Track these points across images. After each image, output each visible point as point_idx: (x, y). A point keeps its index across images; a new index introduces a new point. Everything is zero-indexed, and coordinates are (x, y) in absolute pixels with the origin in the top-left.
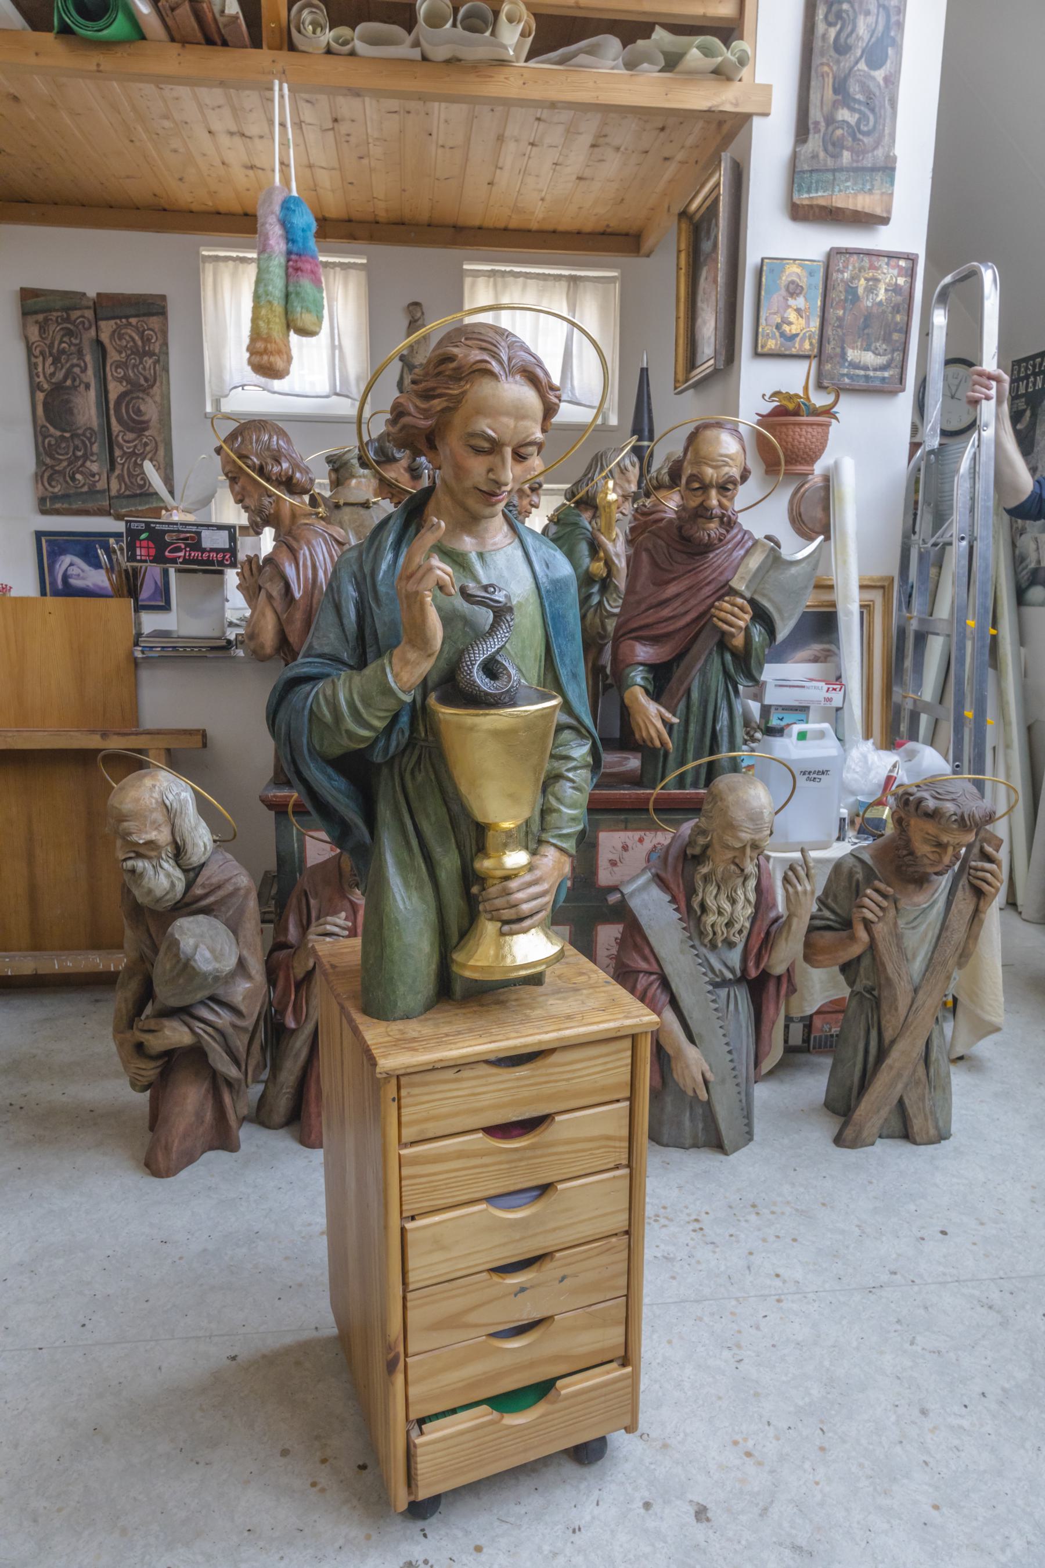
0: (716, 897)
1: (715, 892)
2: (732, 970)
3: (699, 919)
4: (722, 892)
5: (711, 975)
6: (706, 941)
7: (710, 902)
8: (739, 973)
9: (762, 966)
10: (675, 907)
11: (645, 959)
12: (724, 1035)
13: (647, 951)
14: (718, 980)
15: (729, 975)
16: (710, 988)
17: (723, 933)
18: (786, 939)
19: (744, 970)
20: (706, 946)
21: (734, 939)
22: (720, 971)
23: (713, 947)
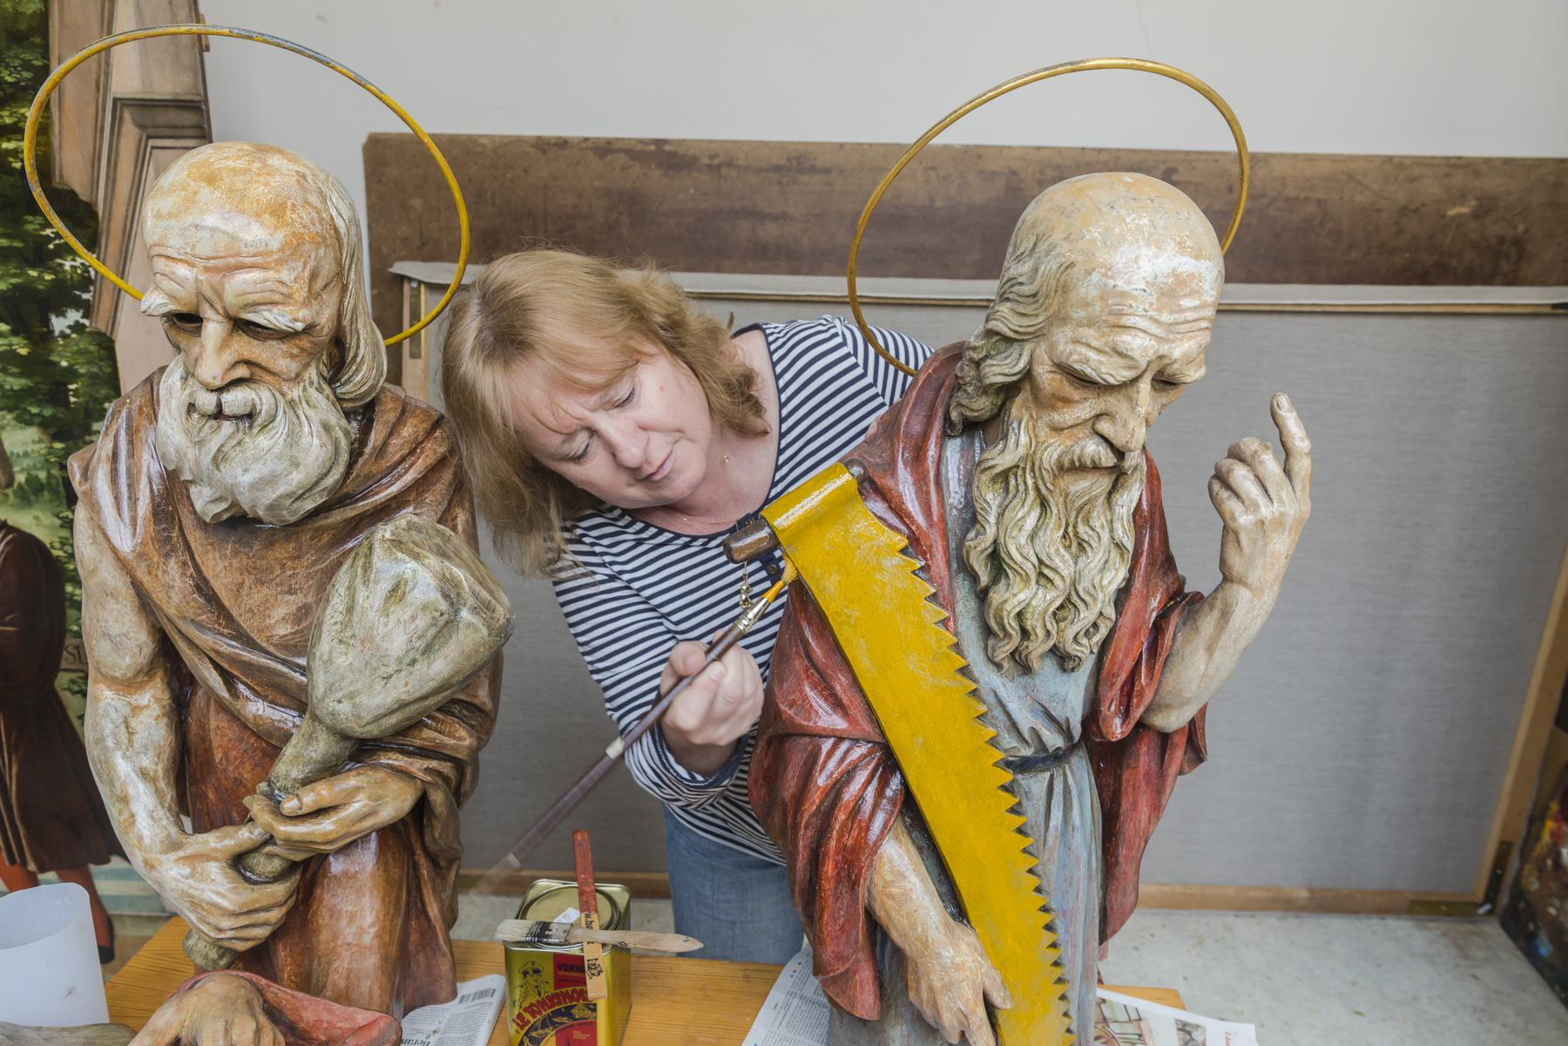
0: (1033, 536)
1: (1030, 522)
3: (982, 596)
4: (1052, 521)
5: (1009, 741)
6: (1003, 652)
7: (1017, 548)
8: (1077, 731)
9: (1137, 714)
10: (919, 564)
11: (838, 705)
12: (1038, 890)
13: (841, 684)
14: (1028, 752)
15: (1054, 741)
16: (1007, 776)
17: (1048, 633)
18: (1210, 649)
19: (1092, 717)
20: (998, 666)
21: (1072, 649)
23: (1024, 667)
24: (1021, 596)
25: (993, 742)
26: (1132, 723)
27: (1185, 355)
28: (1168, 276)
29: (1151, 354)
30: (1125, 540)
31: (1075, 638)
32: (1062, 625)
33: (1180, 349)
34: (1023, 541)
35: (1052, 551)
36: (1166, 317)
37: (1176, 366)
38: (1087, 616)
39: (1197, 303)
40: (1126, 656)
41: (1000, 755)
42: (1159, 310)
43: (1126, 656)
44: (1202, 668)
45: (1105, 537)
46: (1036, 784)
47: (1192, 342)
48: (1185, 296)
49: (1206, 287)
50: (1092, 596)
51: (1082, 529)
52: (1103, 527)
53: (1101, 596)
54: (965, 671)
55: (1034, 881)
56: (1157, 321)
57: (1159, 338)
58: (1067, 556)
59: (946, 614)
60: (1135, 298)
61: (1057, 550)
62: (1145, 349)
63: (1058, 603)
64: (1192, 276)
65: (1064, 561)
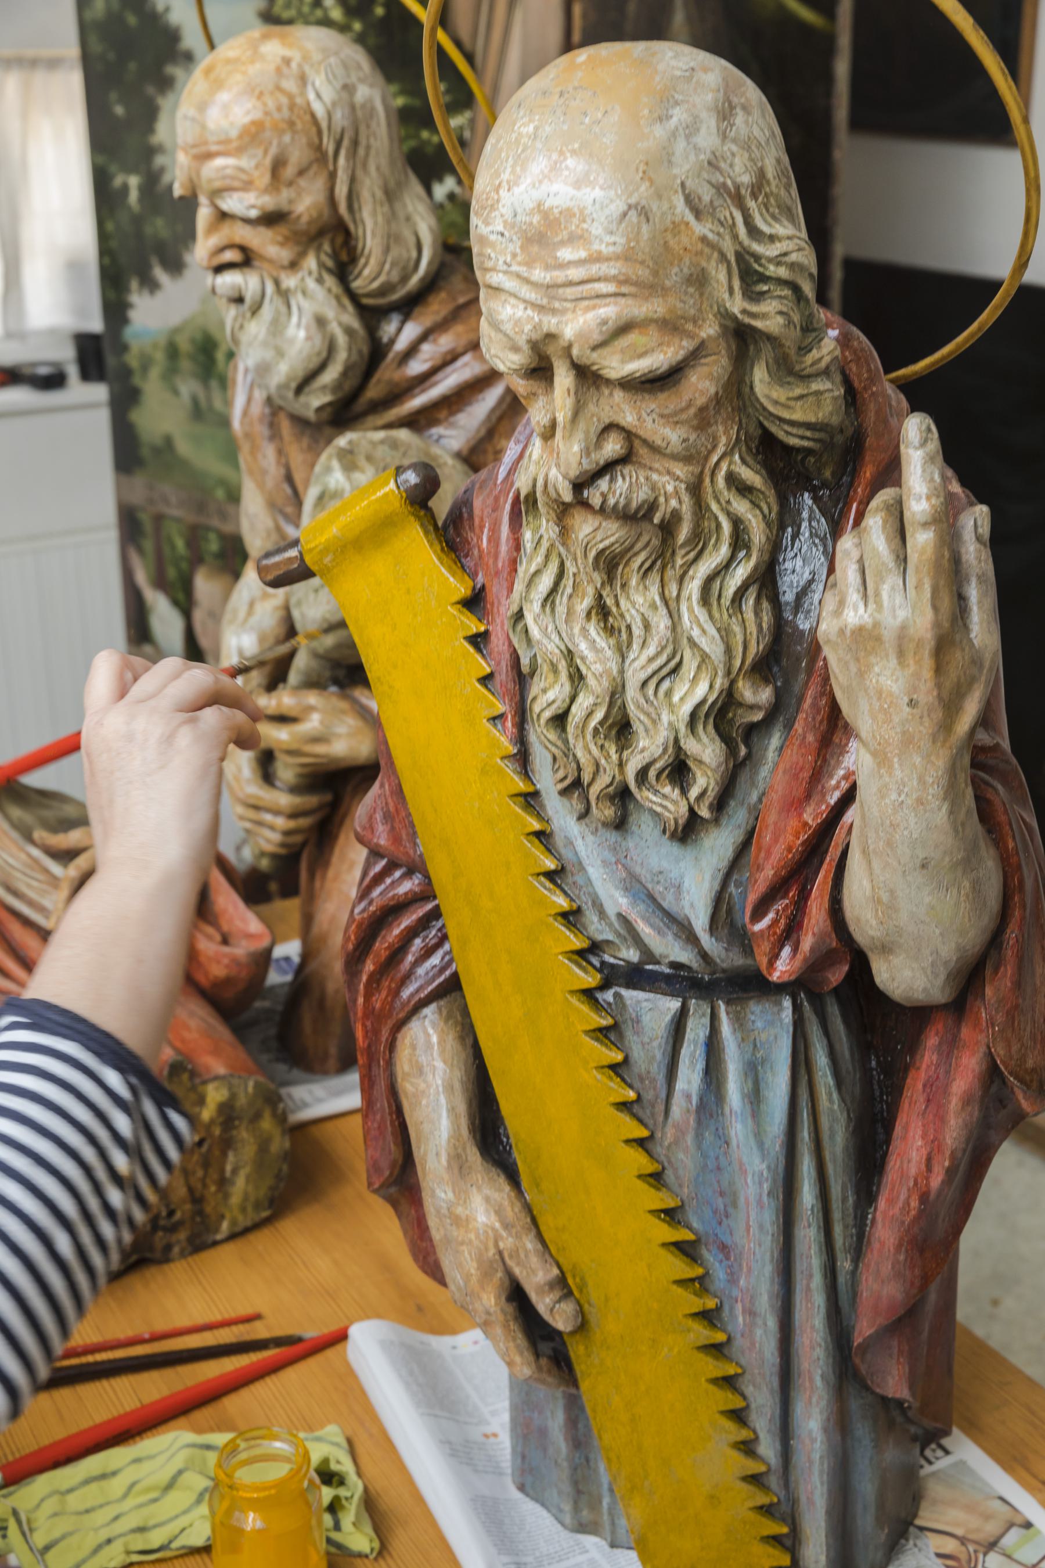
2: (686, 933)
14: (632, 955)
22: (622, 918)
24: (551, 695)
25: (571, 917)
26: (800, 957)
27: (581, 335)
28: (531, 213)
29: (528, 328)
30: (696, 633)
31: (642, 775)
32: (625, 753)
33: (576, 325)
34: (536, 606)
35: (576, 630)
36: (538, 274)
37: (575, 352)
38: (649, 746)
39: (583, 254)
40: (776, 840)
41: (578, 943)
42: (529, 264)
43: (776, 840)
44: (866, 883)
45: (661, 623)
46: (653, 1010)
47: (590, 315)
48: (563, 243)
49: (596, 230)
50: (648, 715)
51: (623, 602)
52: (653, 606)
53: (665, 718)
54: (531, 800)
55: (639, 1161)
56: (527, 281)
57: (541, 308)
58: (601, 642)
59: (500, 708)
60: (492, 245)
61: (584, 631)
62: (518, 322)
63: (599, 715)
64: (568, 213)
65: (597, 651)
